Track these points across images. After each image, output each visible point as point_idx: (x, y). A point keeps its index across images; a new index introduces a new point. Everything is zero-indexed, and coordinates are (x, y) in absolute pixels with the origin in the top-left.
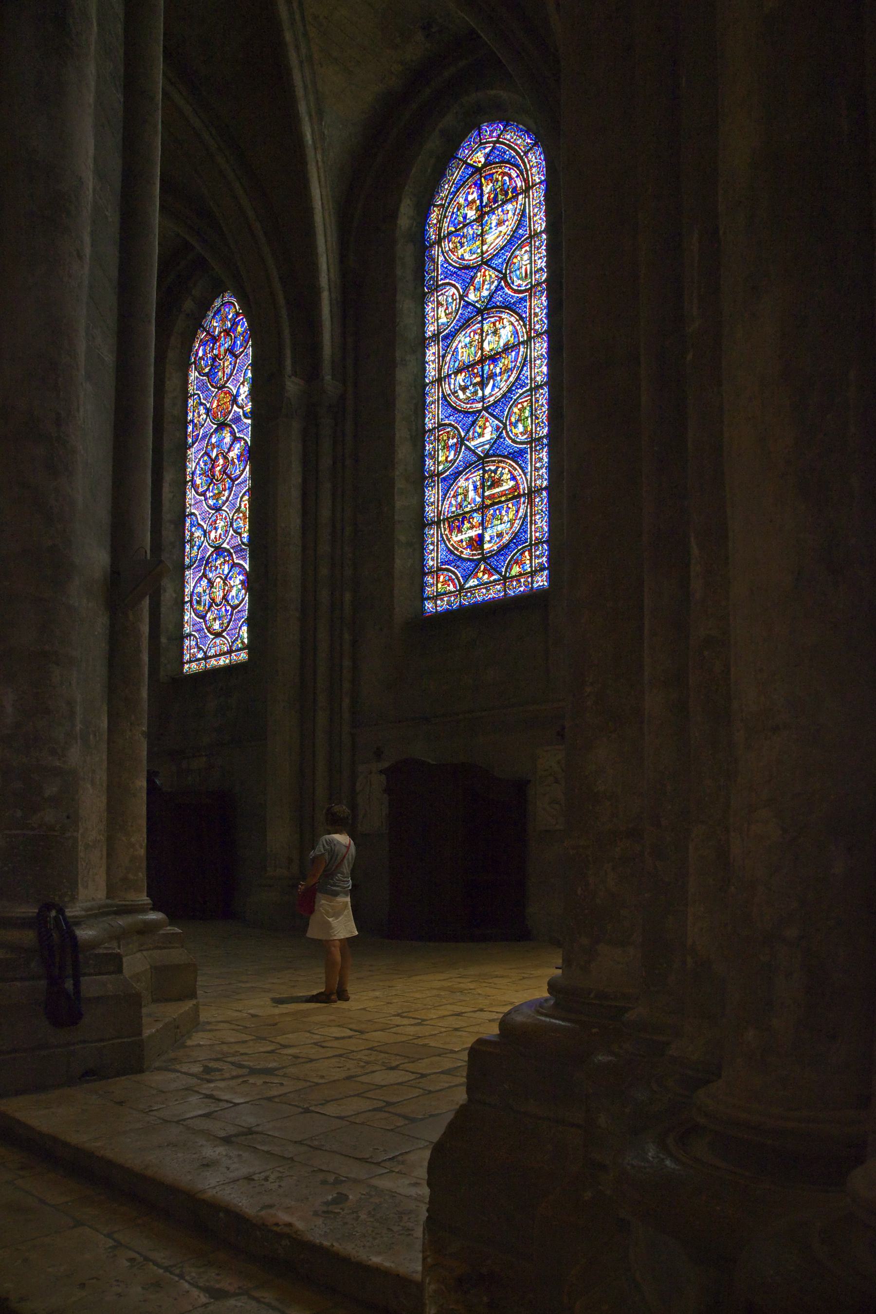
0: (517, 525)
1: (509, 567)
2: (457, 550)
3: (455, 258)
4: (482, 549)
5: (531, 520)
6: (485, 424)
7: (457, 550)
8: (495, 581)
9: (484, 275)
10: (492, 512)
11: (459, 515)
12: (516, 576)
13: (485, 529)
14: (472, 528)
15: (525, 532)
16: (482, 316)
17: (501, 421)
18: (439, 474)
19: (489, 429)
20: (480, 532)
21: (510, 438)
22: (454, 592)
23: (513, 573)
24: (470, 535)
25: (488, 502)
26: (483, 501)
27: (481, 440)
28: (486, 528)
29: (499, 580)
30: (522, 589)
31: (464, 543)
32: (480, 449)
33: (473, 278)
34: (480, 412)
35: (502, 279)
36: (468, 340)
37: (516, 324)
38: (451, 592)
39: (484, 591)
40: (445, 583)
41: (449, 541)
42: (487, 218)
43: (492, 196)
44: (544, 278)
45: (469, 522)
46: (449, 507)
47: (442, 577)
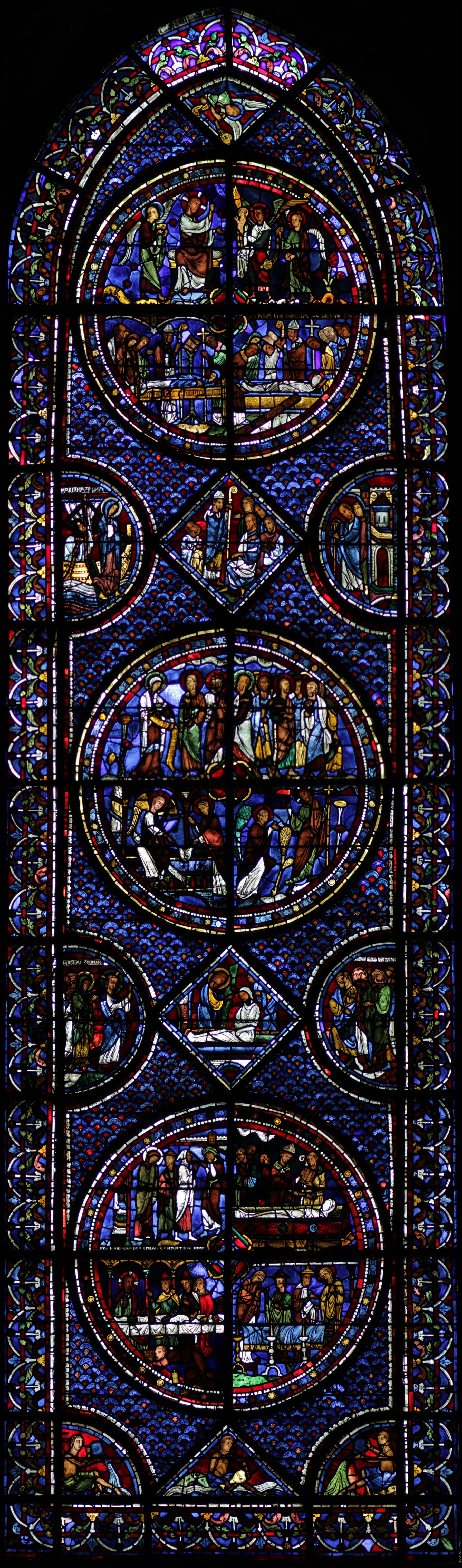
0: (348, 1344)
1: (324, 1465)
2: (135, 1367)
3: (126, 400)
4: (228, 1388)
5: (398, 1338)
6: (236, 989)
7: (135, 1367)
8: (270, 1495)
9: (238, 507)
10: (259, 1277)
11: (140, 1254)
12: (343, 1498)
13: (235, 1325)
14: (190, 1308)
15: (380, 1371)
16: (230, 641)
17: (295, 1001)
18: (66, 1099)
19: (251, 1012)
20: (220, 1329)
21: (325, 1062)
22: (123, 1499)
23: (336, 1485)
24: (184, 1329)
25: (245, 1241)
26: (227, 1233)
27: (225, 1036)
28: (243, 1323)
29: (287, 1498)
30: (368, 1544)
31: (160, 1353)
32: (216, 1063)
33: (196, 499)
34: (219, 943)
35: (301, 548)
36: (175, 693)
37: (350, 714)
38: (113, 1498)
39: (235, 1519)
40: (87, 1462)
41: (104, 1333)
42: (247, 327)
43: (268, 264)
44: (441, 611)
45: (179, 1289)
46: (103, 1217)
47: (77, 1444)
